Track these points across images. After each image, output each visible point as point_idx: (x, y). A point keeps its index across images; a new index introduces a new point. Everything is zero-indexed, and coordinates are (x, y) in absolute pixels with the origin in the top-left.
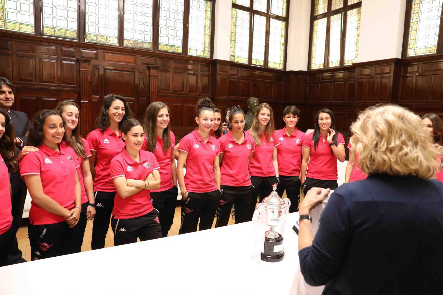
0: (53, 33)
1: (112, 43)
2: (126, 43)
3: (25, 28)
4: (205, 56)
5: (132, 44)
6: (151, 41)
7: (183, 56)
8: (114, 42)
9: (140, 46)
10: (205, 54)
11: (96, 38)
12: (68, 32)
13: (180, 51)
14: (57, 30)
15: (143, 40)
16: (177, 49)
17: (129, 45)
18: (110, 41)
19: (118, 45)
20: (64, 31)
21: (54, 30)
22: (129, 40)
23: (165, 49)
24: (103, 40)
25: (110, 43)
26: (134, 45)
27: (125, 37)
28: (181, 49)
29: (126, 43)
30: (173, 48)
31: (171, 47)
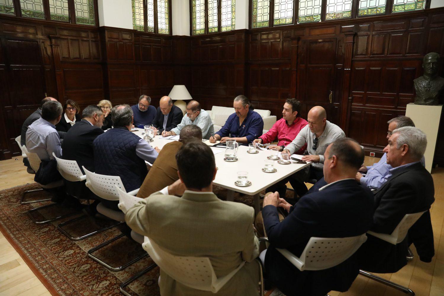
0: (279, 23)
1: (316, 20)
2: (328, 17)
3: (265, 24)
4: (417, 8)
5: (332, 17)
6: (351, 9)
7: (387, 15)
8: (318, 19)
9: (340, 16)
10: (418, 5)
11: (305, 19)
12: (287, 20)
13: (383, 11)
14: (281, 20)
15: (343, 10)
16: (379, 10)
17: (330, 19)
18: (315, 19)
19: (320, 21)
20: (285, 20)
21: (279, 21)
22: (330, 14)
23: (365, 13)
24: (309, 20)
25: (315, 21)
26: (334, 17)
27: (327, 12)
28: (384, 8)
29: (328, 17)
30: (375, 10)
31: (372, 10)
